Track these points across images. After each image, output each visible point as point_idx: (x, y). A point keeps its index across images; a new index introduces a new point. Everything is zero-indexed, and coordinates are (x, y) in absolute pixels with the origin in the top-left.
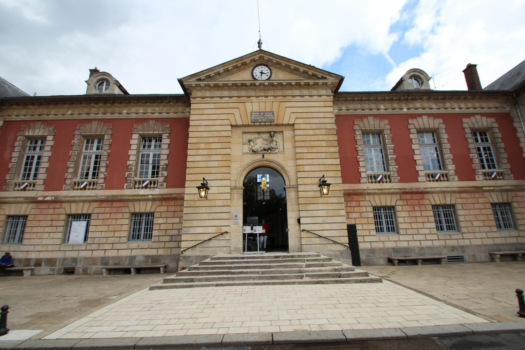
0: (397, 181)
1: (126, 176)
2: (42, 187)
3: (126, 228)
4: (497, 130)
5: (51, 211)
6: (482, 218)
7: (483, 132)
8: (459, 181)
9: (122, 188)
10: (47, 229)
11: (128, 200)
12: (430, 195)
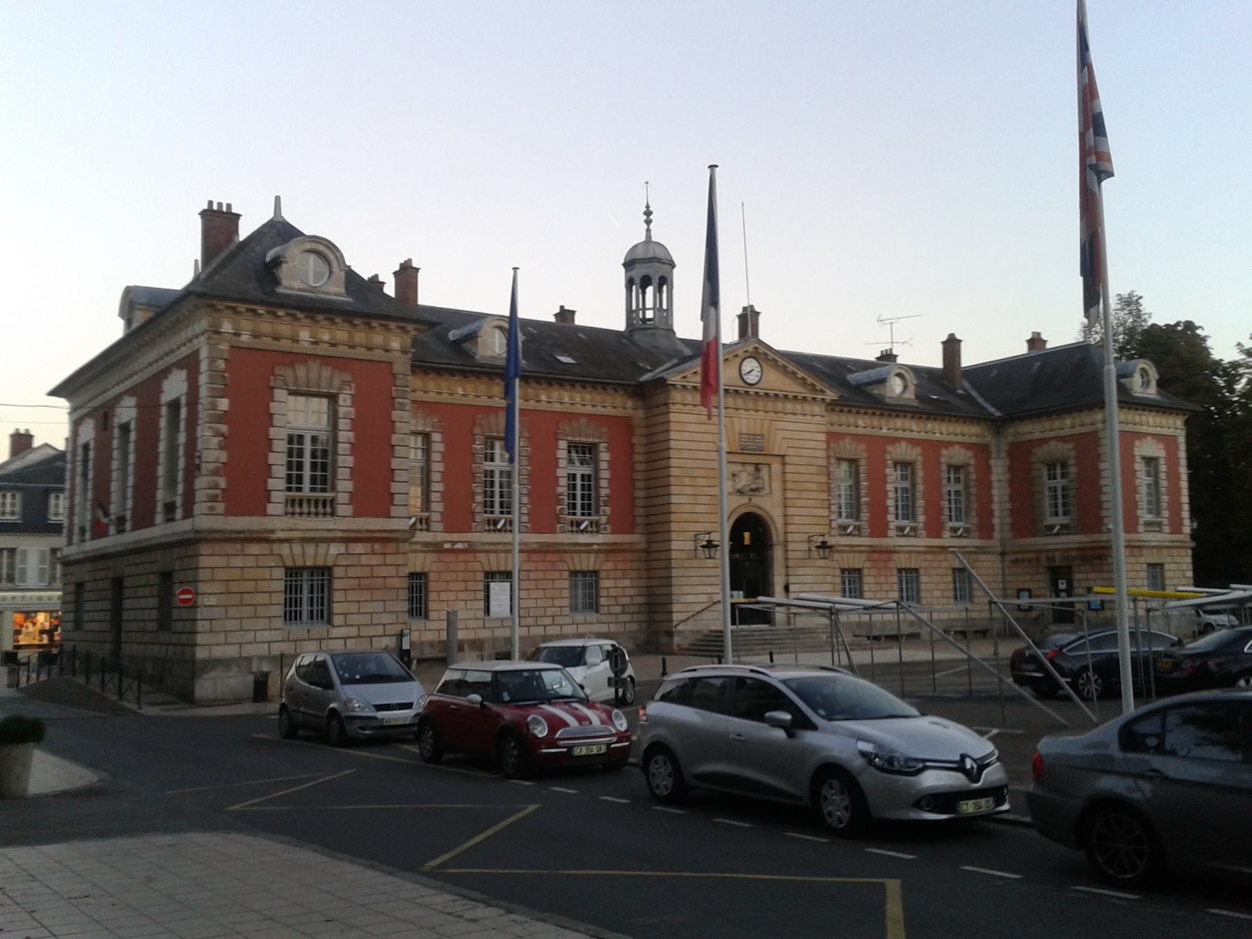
0: (866, 534)
1: (558, 512)
2: (439, 526)
4: (972, 469)
5: (461, 566)
6: (942, 586)
7: (956, 468)
8: (927, 537)
9: (554, 532)
10: (462, 595)
11: (565, 552)
12: (896, 555)
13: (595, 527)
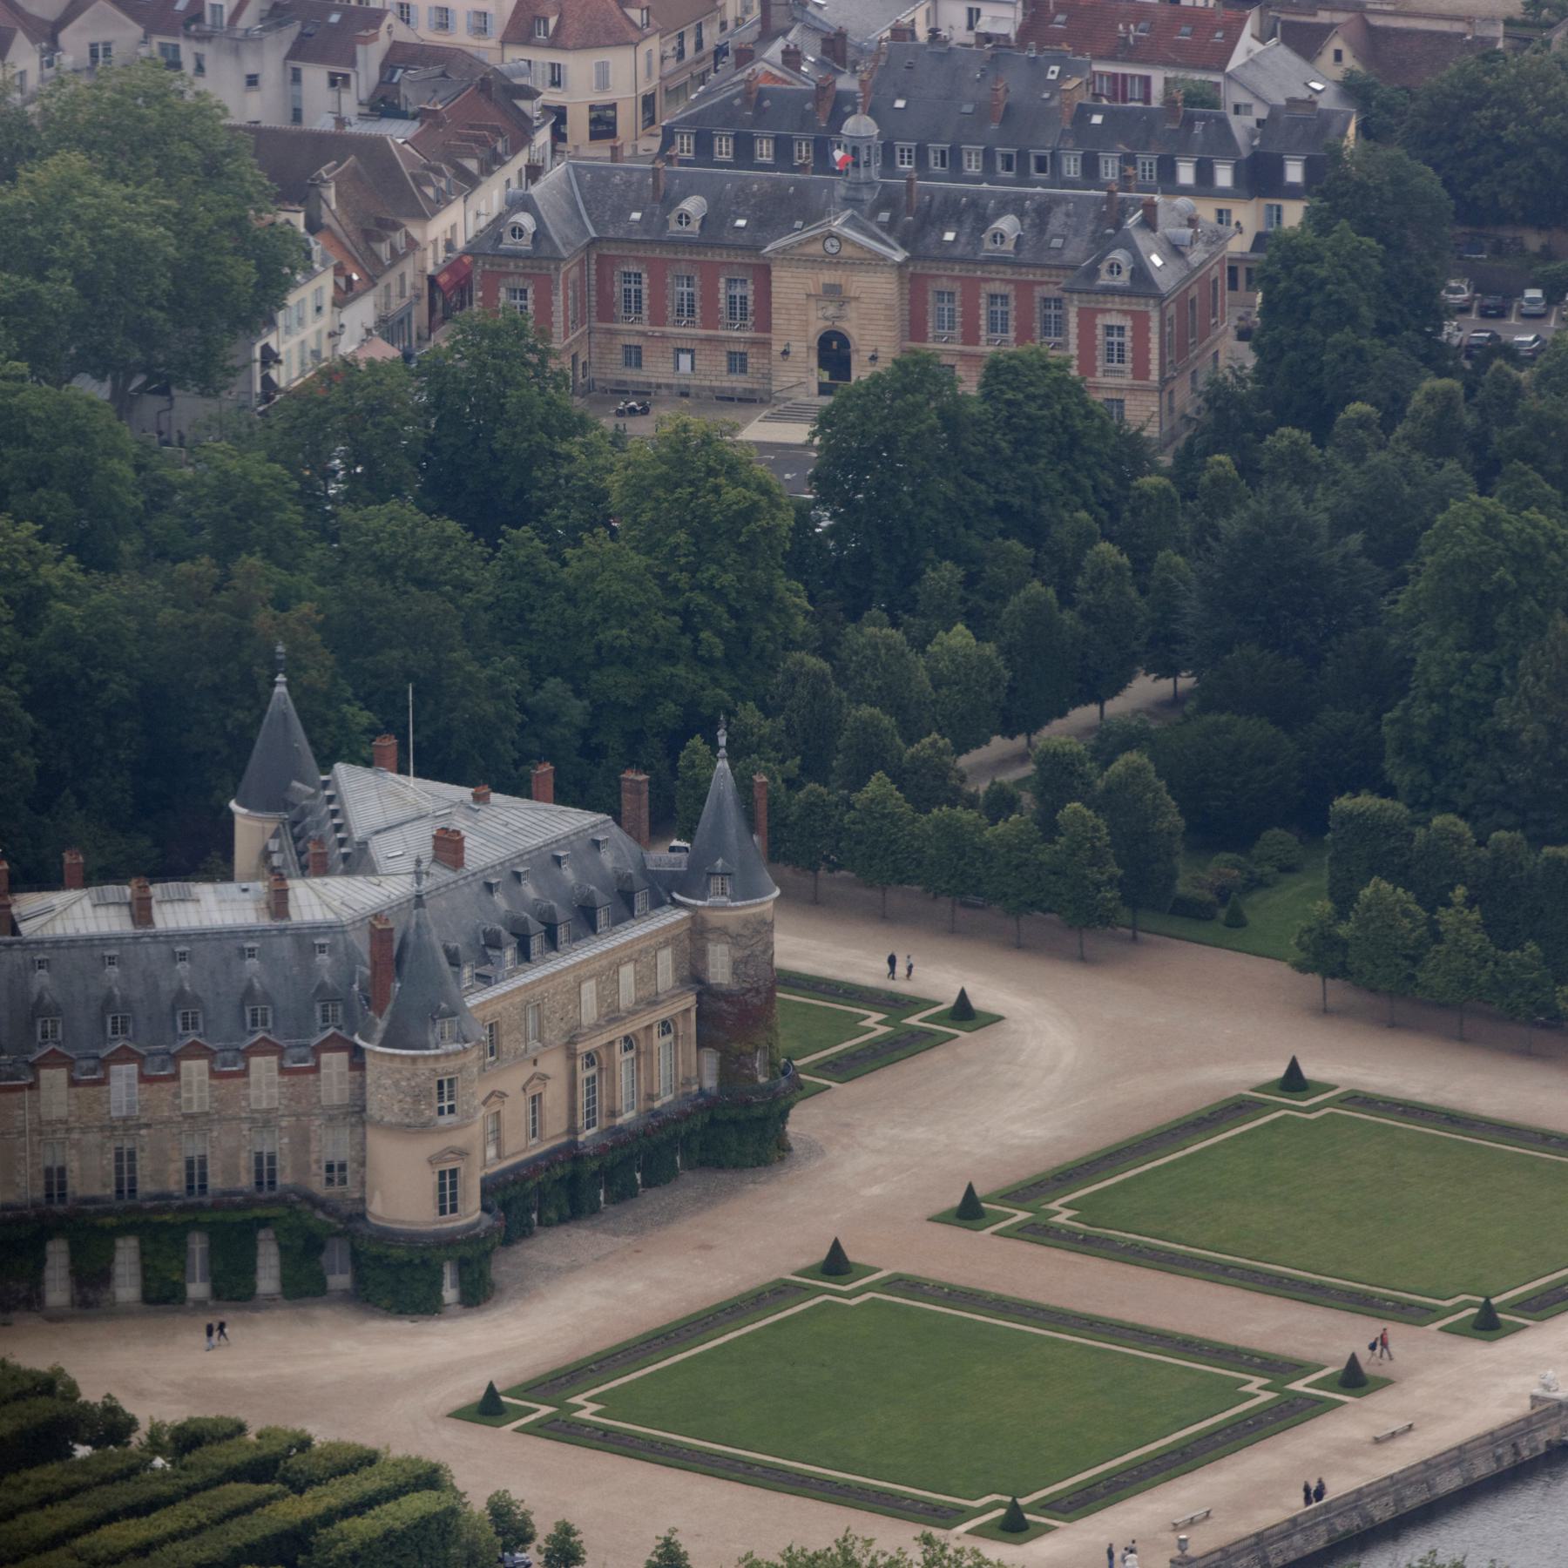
3: (725, 364)
13: (742, 327)
